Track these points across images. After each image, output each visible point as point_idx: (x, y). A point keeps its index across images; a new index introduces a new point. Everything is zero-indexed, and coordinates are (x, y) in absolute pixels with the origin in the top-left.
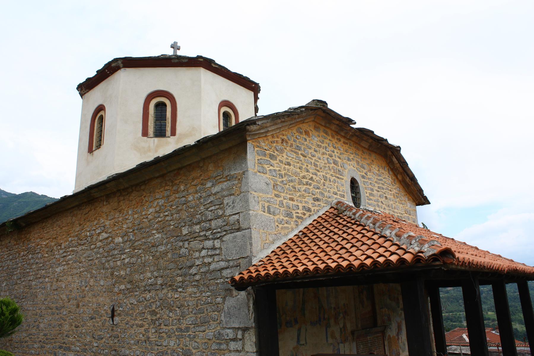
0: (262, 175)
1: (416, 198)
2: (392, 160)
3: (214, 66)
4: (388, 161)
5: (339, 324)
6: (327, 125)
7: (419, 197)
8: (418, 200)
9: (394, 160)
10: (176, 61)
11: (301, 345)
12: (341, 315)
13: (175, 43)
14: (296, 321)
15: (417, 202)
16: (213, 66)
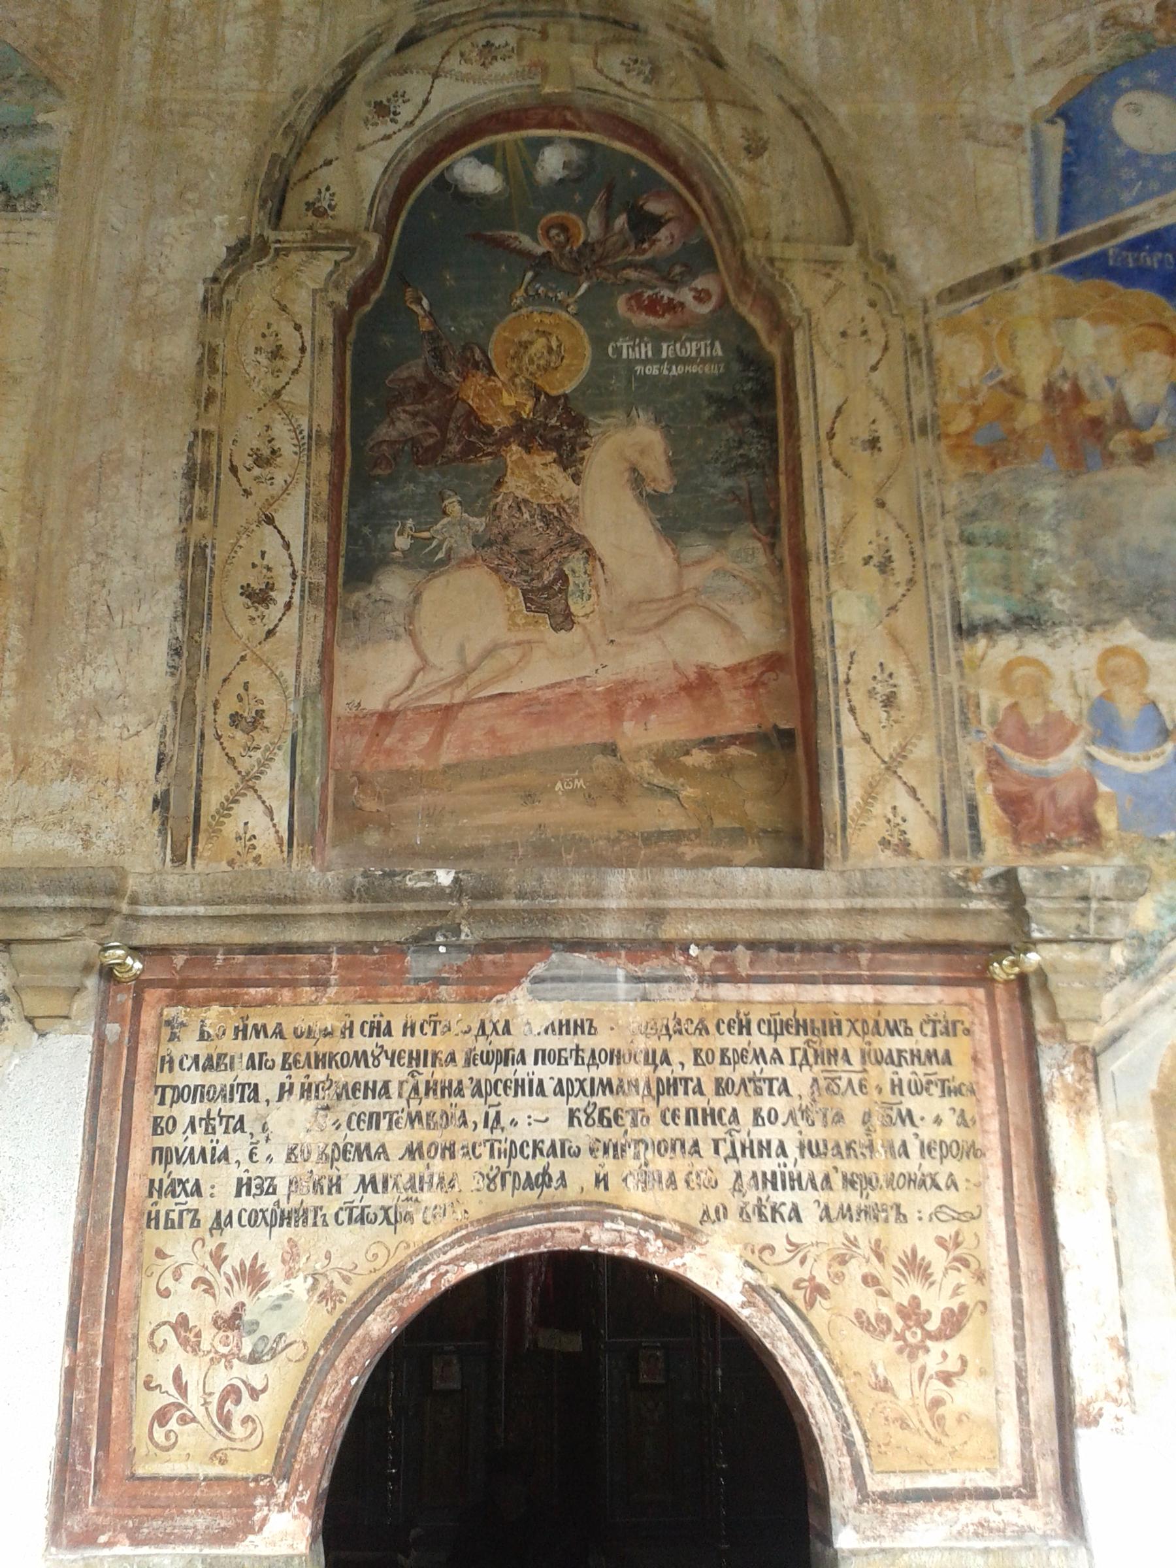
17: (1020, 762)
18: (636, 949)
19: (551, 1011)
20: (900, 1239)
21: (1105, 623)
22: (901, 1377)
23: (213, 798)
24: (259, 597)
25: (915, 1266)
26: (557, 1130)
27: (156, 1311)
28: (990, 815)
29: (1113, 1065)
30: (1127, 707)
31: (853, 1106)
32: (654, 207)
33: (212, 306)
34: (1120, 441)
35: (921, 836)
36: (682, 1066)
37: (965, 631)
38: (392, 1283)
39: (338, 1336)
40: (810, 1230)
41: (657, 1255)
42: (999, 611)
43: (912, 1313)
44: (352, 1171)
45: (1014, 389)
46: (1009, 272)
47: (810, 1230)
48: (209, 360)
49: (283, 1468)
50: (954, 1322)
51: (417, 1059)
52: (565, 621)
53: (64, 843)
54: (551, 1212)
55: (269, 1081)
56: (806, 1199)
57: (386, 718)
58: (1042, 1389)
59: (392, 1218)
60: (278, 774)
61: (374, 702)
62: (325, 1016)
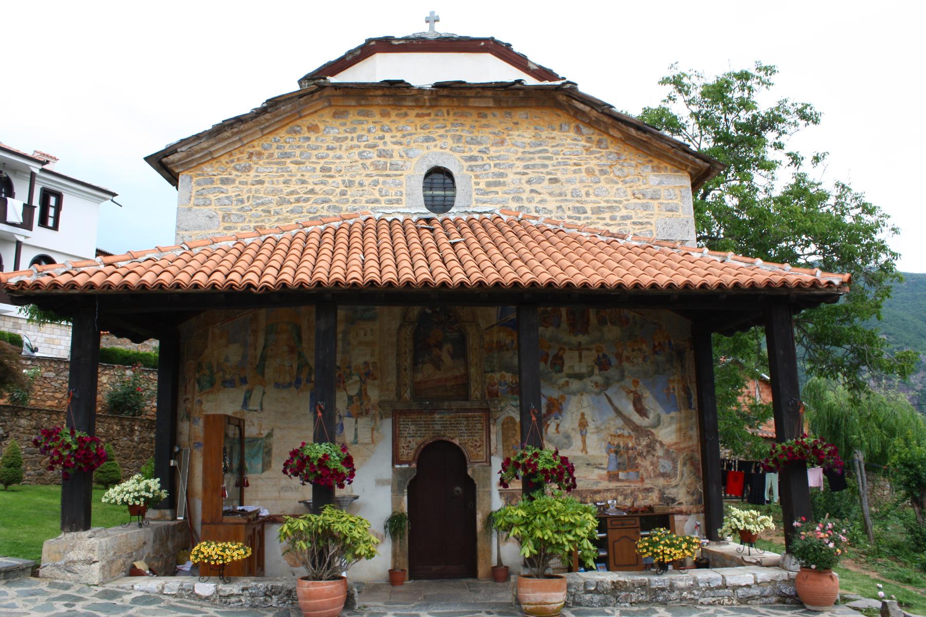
0: (202, 208)
1: (680, 163)
2: (579, 109)
3: (396, 43)
4: (572, 113)
5: (345, 389)
6: (363, 102)
7: (687, 159)
8: (687, 166)
9: (581, 106)
10: (350, 57)
11: (250, 410)
12: (356, 378)
13: (432, 13)
14: (244, 381)
15: (689, 169)
16: (395, 45)
17: (491, 388)
18: (448, 410)
19: (439, 416)
20: (475, 438)
21: (501, 371)
22: (474, 451)
23: (402, 393)
24: (405, 370)
25: (476, 441)
26: (440, 428)
27: (400, 445)
28: (487, 394)
29: (498, 421)
30: (503, 381)
31: (471, 425)
32: (451, 314)
33: (398, 333)
34: (505, 348)
35: (479, 396)
36: (453, 422)
37: (486, 372)
38: (424, 443)
39: (418, 448)
40: (466, 438)
41: (450, 440)
42: (489, 370)
43: (476, 445)
44: (419, 432)
45: (492, 342)
46: (493, 326)
47: (466, 438)
48: (398, 340)
49: (414, 460)
50: (480, 446)
51: (425, 421)
52: (440, 370)
53: (387, 398)
54: (439, 436)
55: (410, 423)
56: (466, 435)
57: (419, 383)
58: (488, 452)
59: (423, 437)
60: (409, 391)
61: (418, 380)
62: (415, 417)
